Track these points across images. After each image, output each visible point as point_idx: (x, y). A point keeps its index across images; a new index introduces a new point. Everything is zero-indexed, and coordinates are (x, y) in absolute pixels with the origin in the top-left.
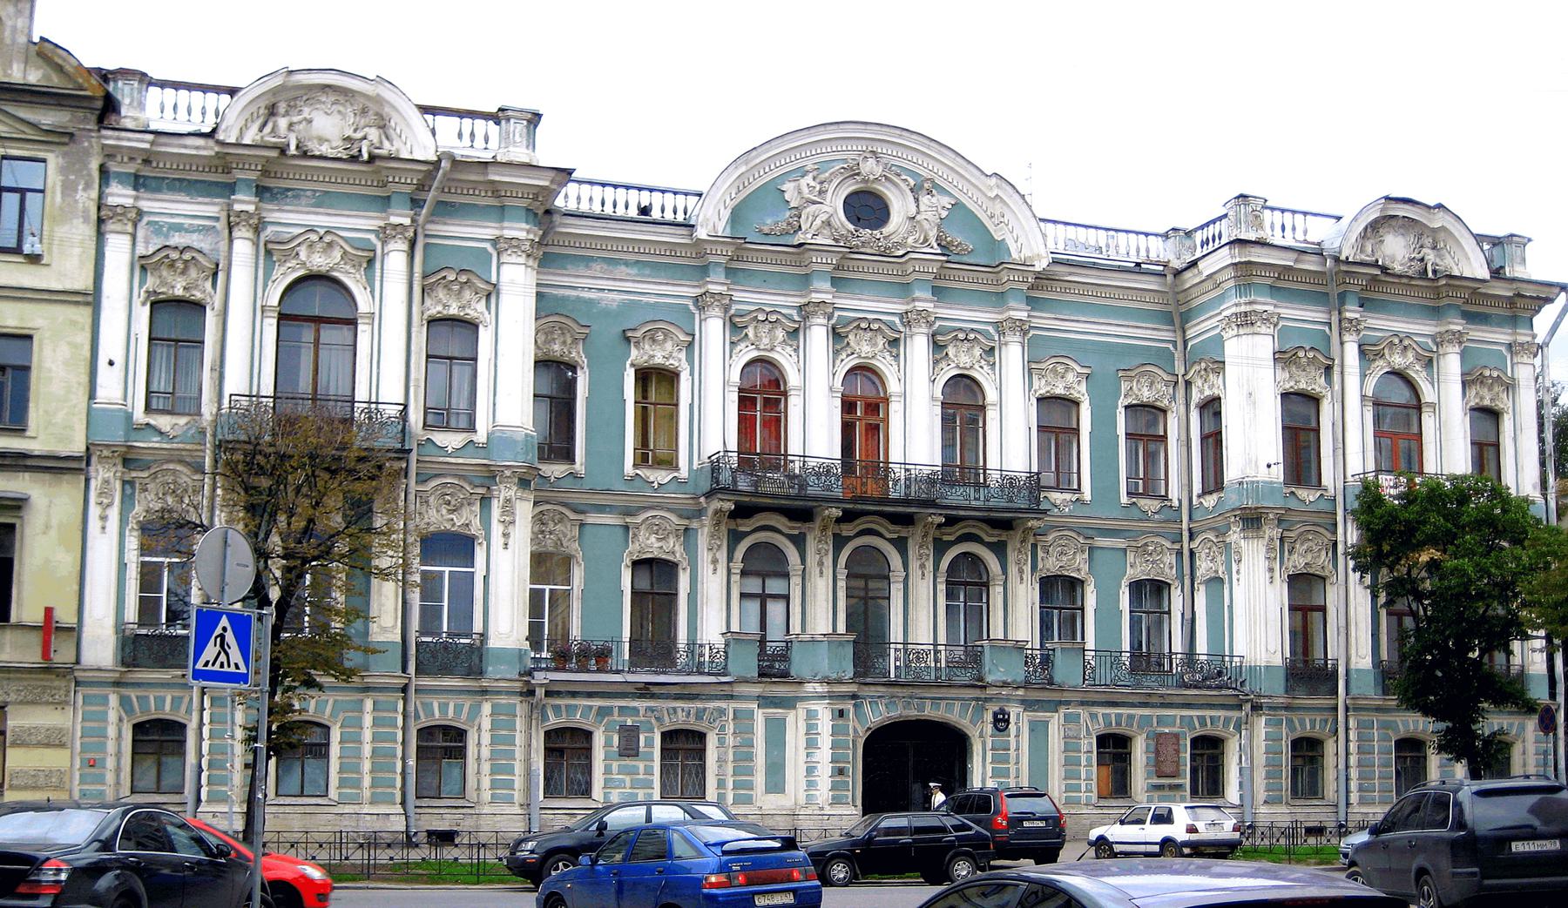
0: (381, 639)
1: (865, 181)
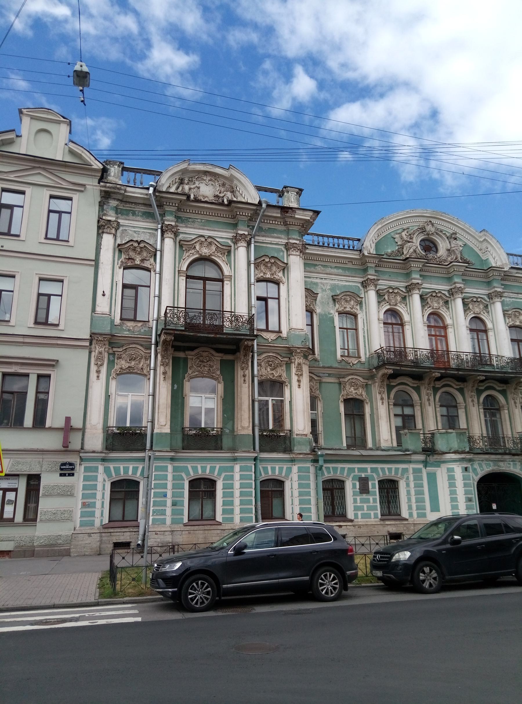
0: (243, 433)
1: (428, 234)
